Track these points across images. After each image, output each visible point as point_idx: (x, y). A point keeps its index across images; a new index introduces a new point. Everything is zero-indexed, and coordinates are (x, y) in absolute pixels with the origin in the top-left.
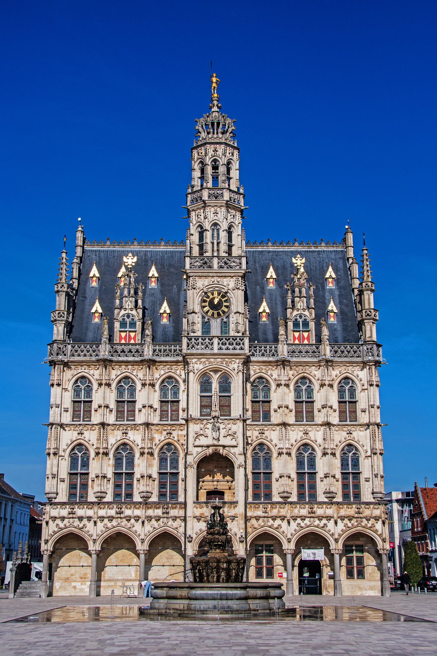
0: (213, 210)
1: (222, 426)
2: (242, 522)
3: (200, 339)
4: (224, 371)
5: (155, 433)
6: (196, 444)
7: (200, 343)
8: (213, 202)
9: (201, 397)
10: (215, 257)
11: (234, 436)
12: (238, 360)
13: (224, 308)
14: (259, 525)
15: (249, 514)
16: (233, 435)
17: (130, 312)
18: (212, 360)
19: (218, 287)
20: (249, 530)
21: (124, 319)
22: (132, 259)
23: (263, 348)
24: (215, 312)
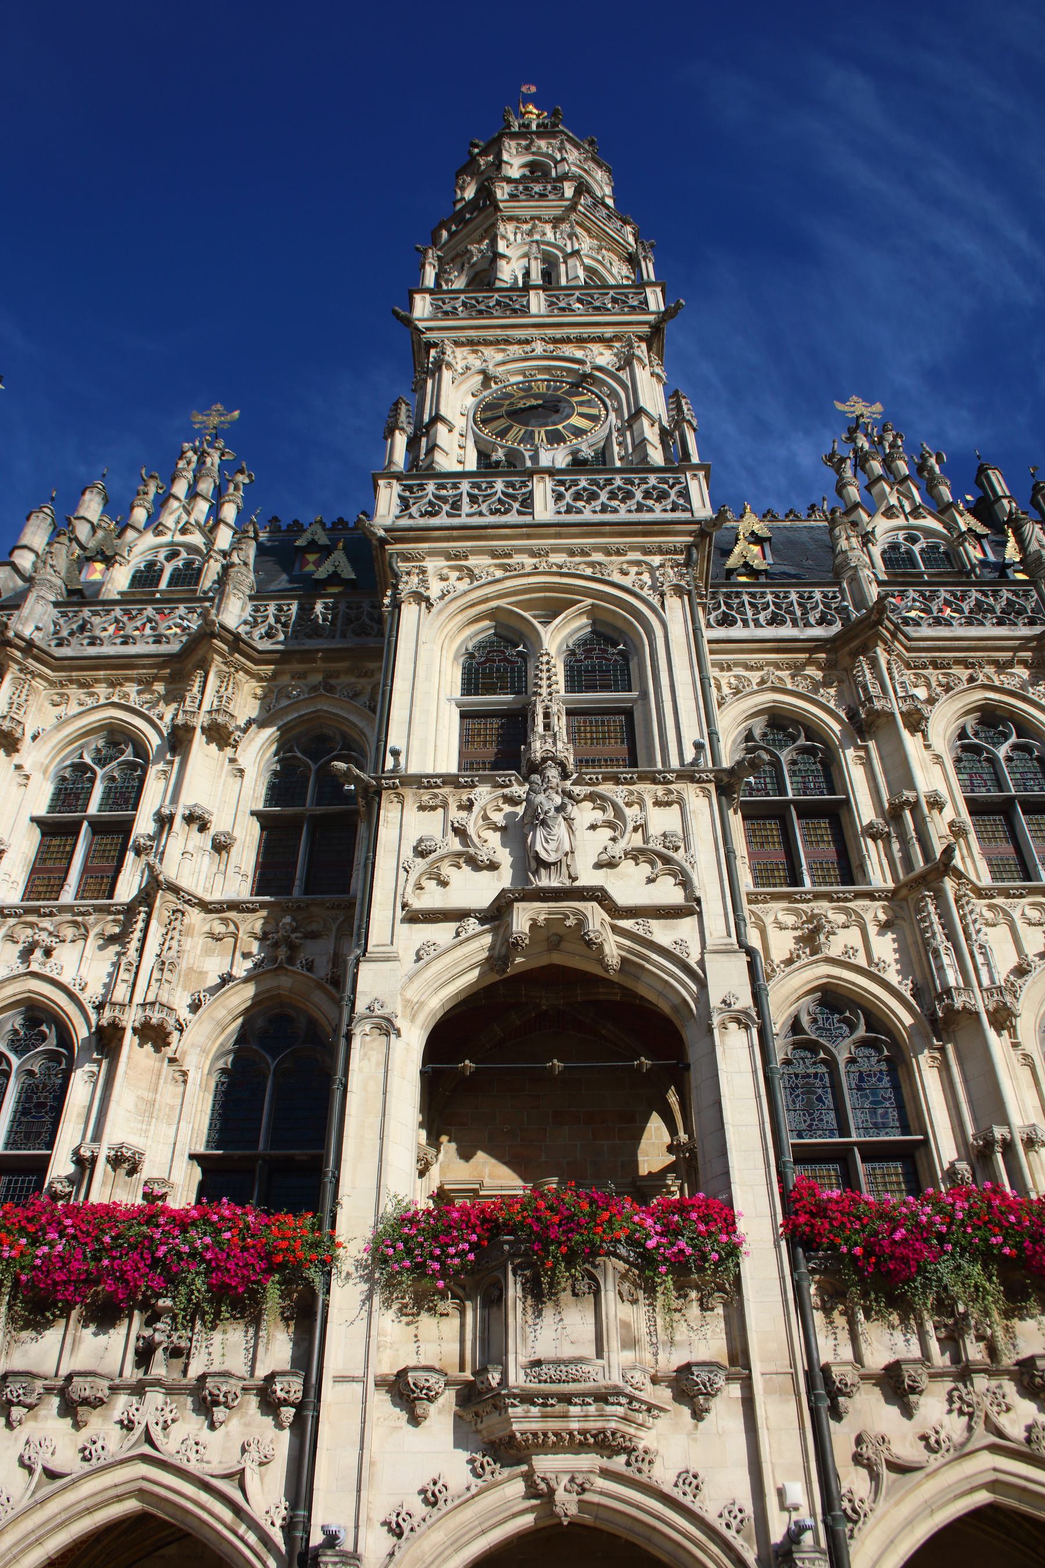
0: (526, 227)
1: (585, 814)
2: (781, 1418)
3: (465, 486)
4: (590, 601)
5: (207, 952)
6: (420, 902)
7: (466, 499)
8: (525, 208)
9: (464, 715)
10: (536, 287)
11: (667, 860)
12: (656, 560)
13: (576, 421)
14: (930, 1443)
15: (832, 1348)
16: (663, 858)
17: (179, 538)
18: (529, 561)
19: (547, 369)
20: (854, 1482)
21: (151, 565)
22: (221, 415)
23: (769, 598)
24: (536, 430)
